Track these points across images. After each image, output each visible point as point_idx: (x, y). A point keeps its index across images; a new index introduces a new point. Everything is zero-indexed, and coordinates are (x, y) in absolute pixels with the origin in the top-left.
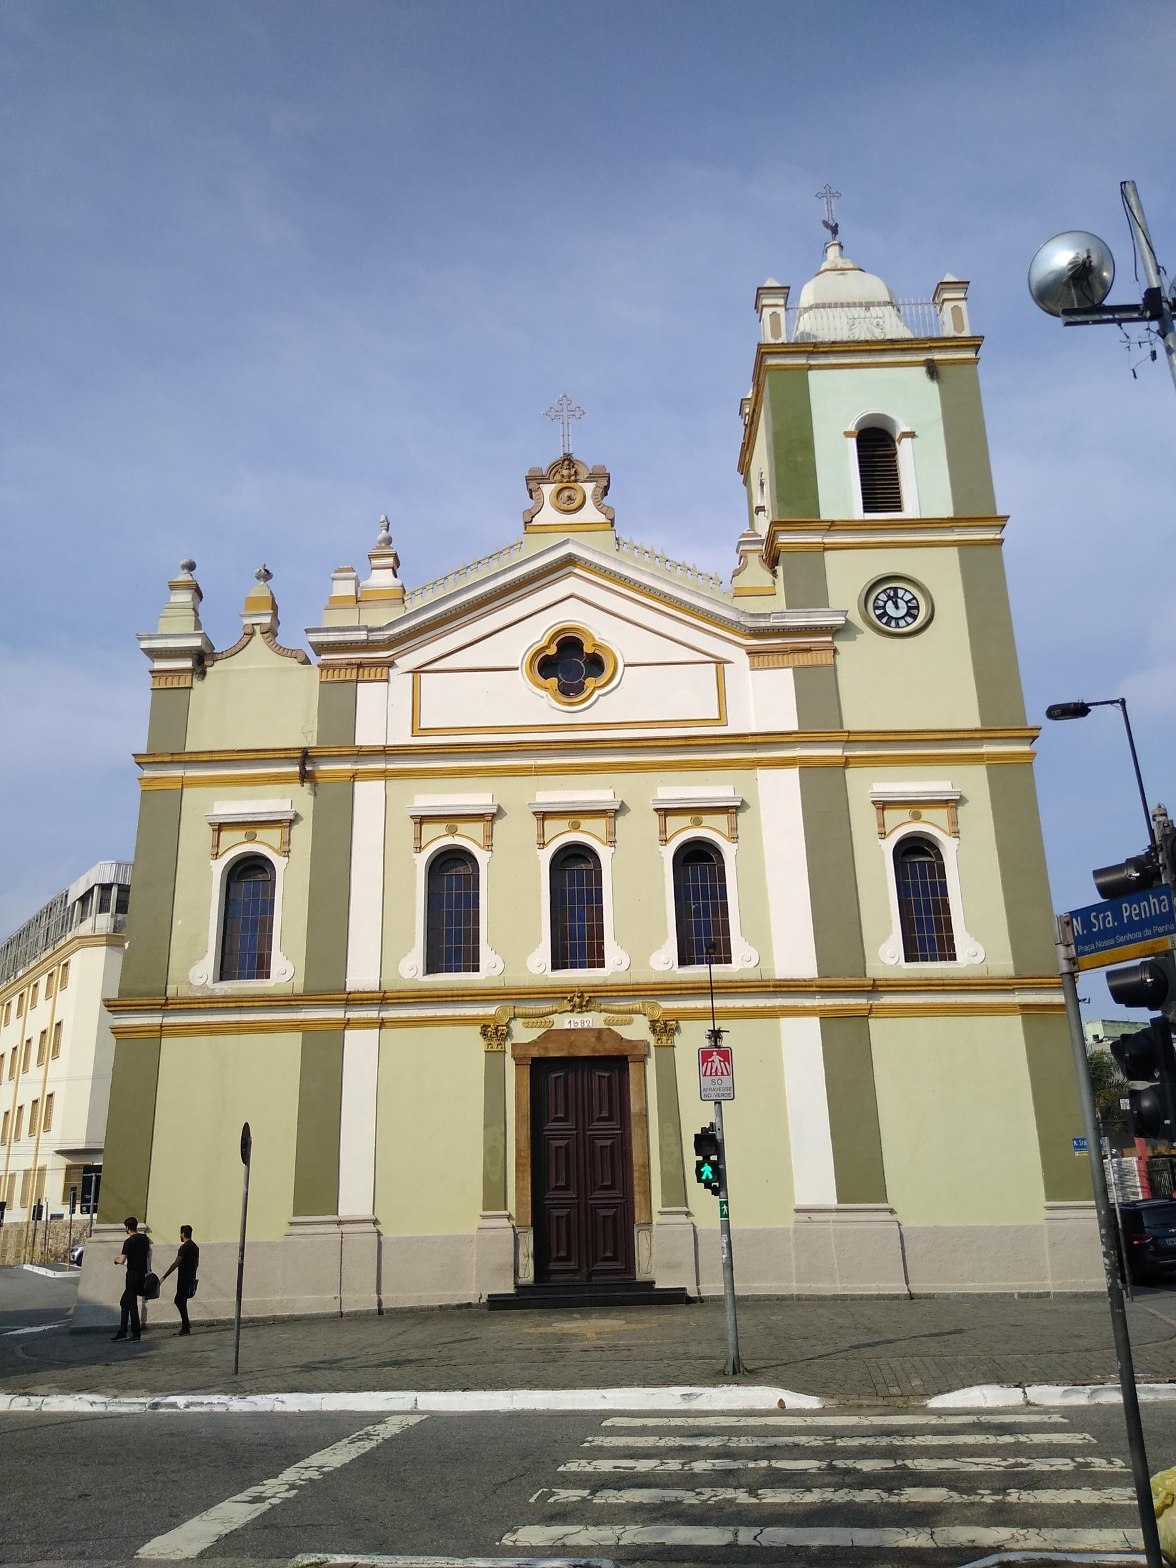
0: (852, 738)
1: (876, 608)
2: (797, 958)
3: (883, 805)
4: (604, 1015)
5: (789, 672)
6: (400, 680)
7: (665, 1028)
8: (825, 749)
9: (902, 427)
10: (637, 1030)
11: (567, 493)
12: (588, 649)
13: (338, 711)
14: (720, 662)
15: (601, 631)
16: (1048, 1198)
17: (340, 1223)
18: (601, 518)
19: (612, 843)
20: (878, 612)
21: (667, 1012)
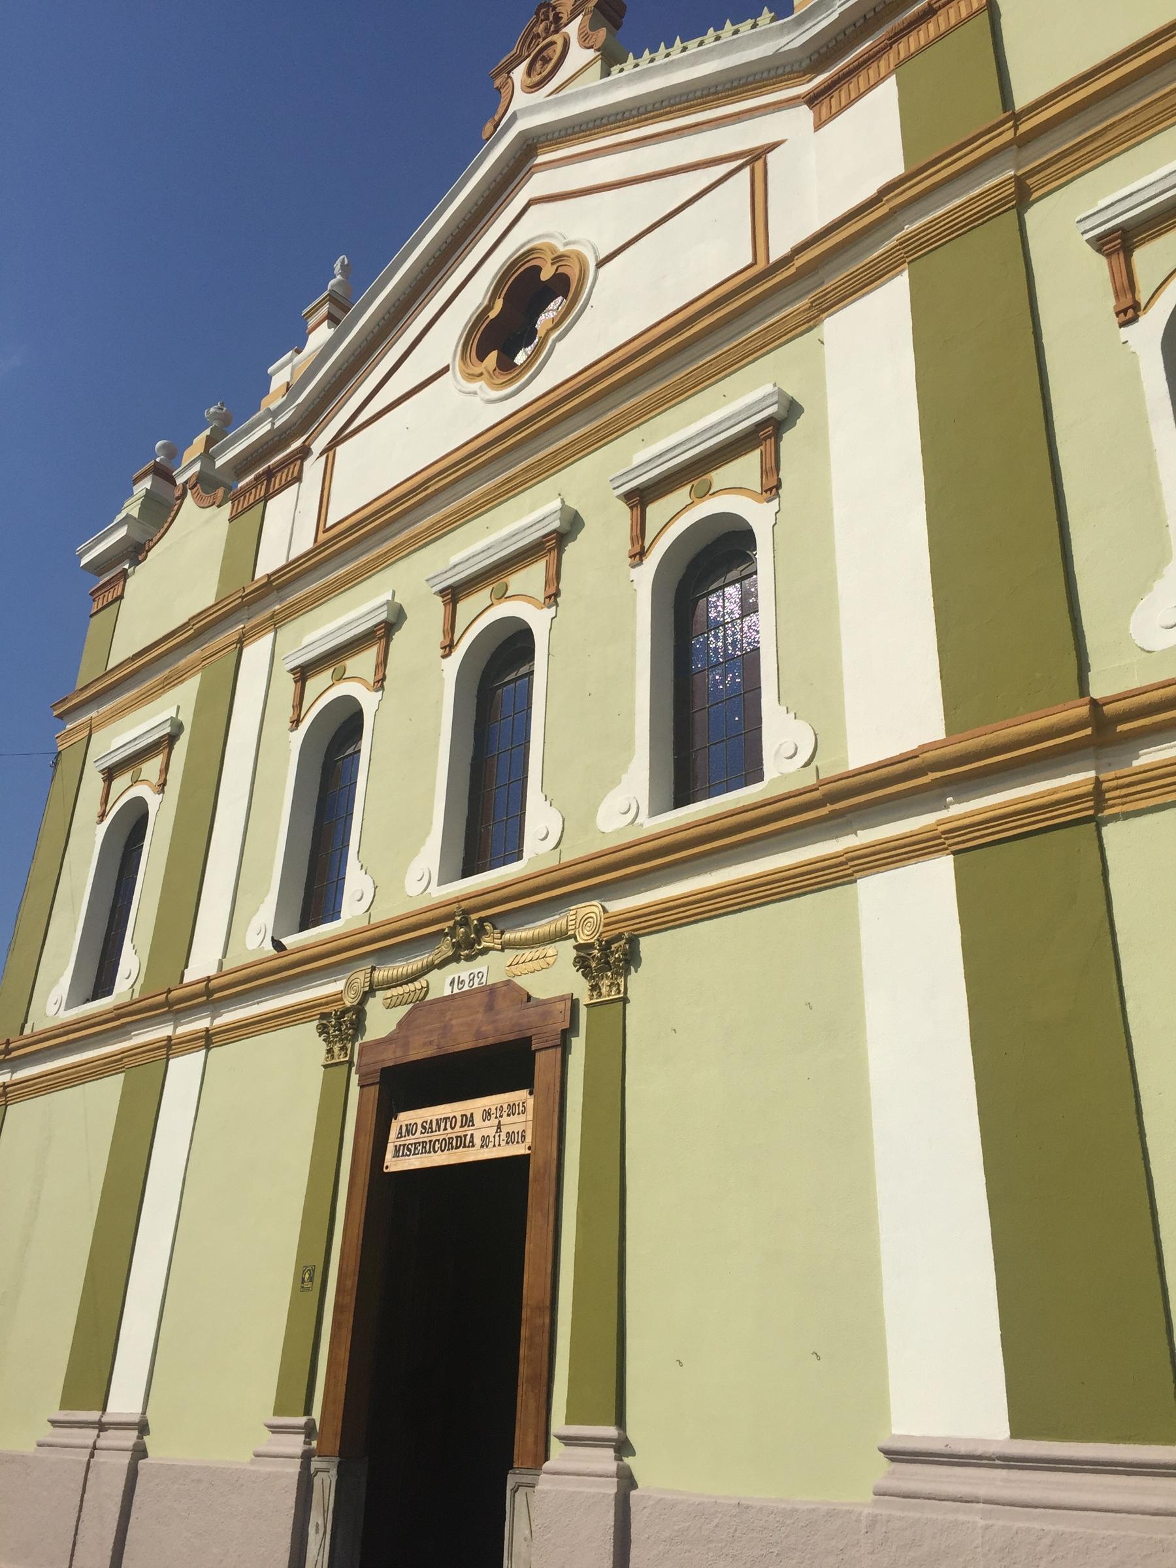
0: (1024, 128)
7: (610, 958)
10: (553, 976)
17: (102, 1427)
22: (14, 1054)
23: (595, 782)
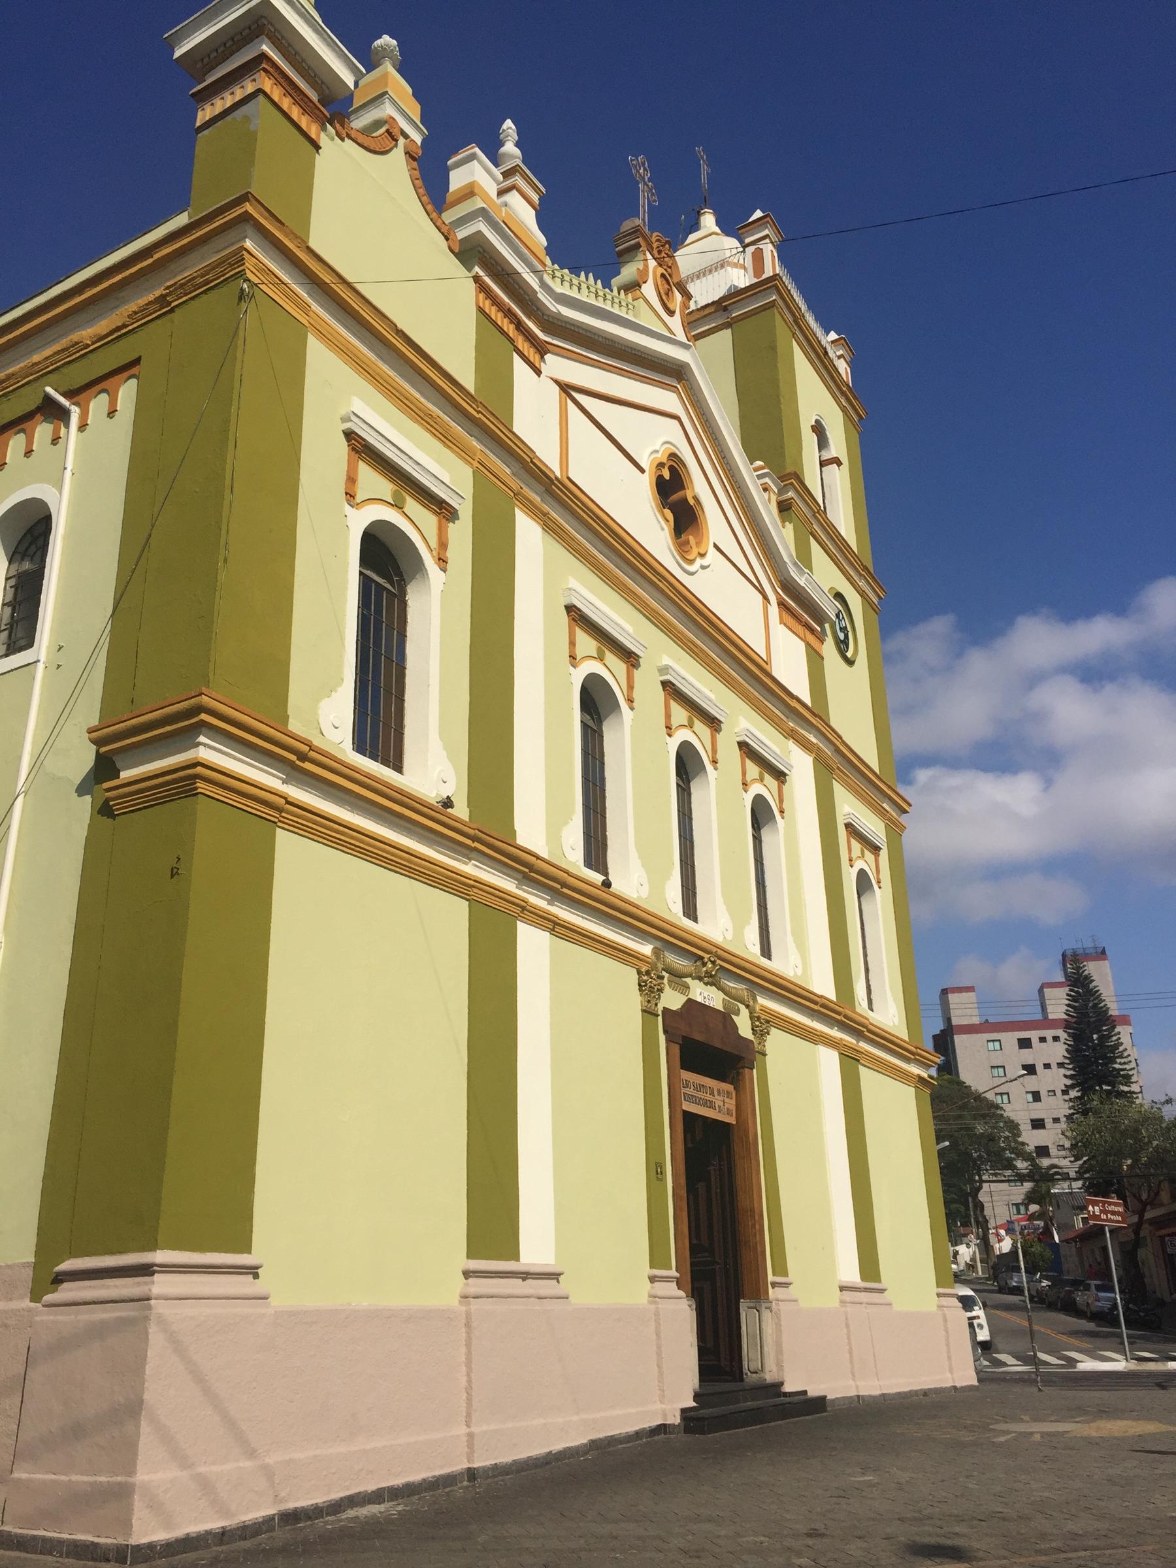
4: (721, 995)
14: (765, 597)
17: (525, 1276)
21: (764, 1009)
22: (308, 766)
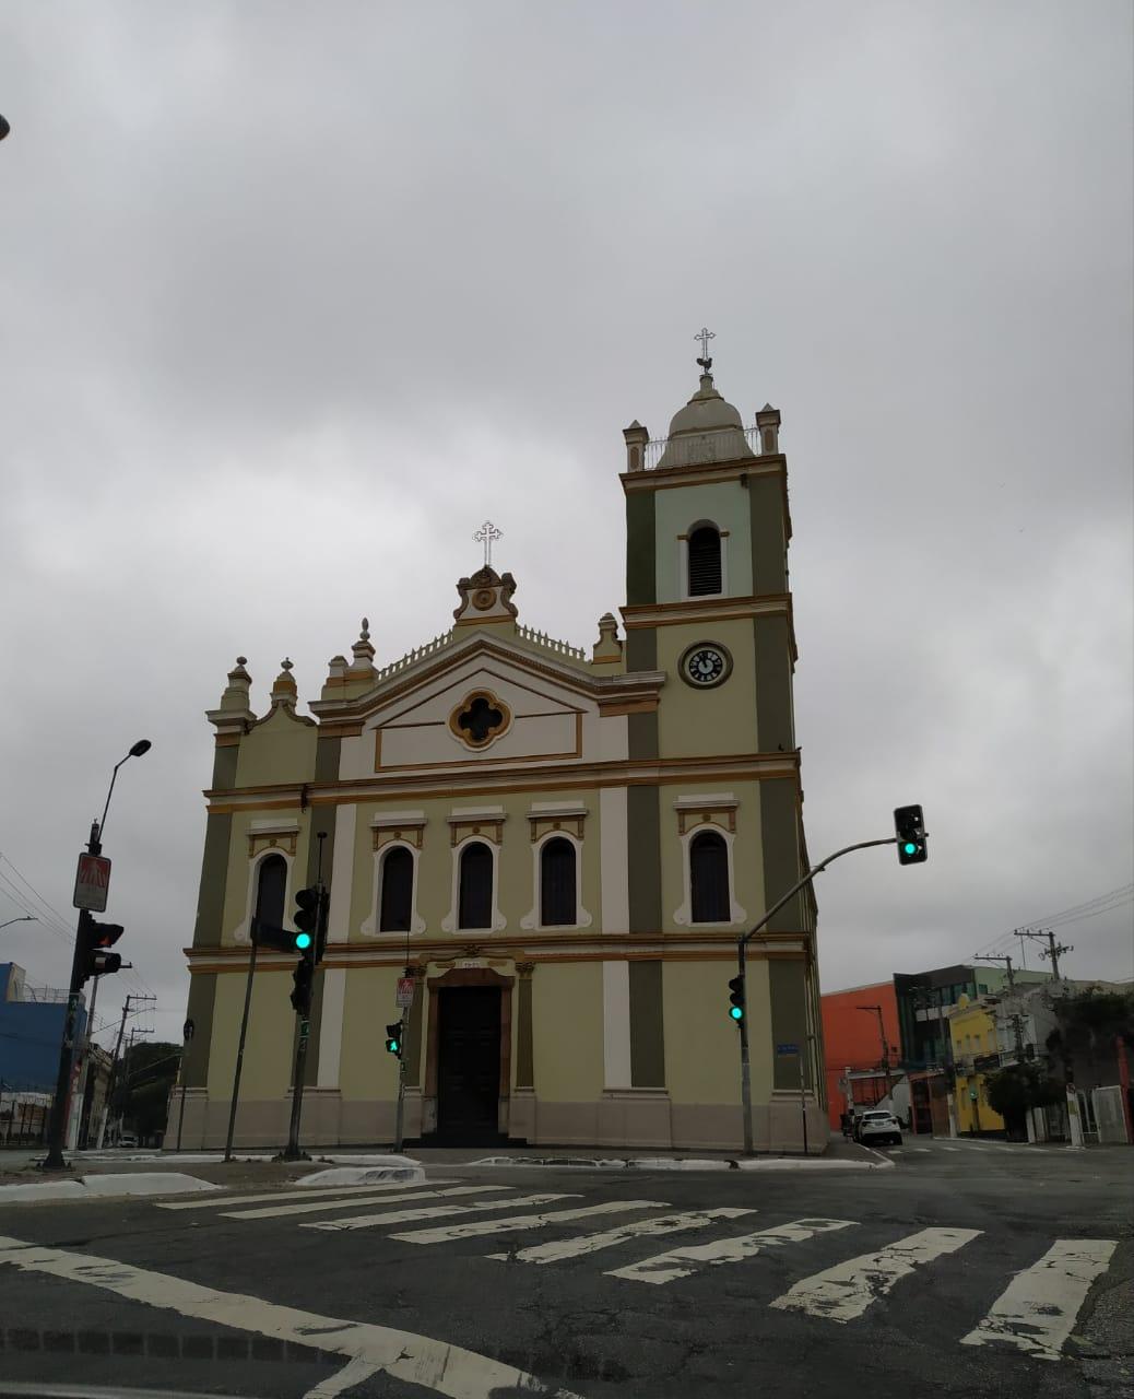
1: (691, 667)
2: (616, 920)
3: (683, 812)
5: (624, 719)
6: (368, 734)
7: (526, 968)
8: (645, 777)
9: (722, 530)
10: (507, 970)
11: (483, 596)
12: (491, 707)
13: (328, 756)
14: (579, 712)
15: (502, 694)
16: (776, 1087)
17: (318, 1091)
18: (506, 612)
19: (499, 842)
20: (692, 670)
23: (516, 908)
